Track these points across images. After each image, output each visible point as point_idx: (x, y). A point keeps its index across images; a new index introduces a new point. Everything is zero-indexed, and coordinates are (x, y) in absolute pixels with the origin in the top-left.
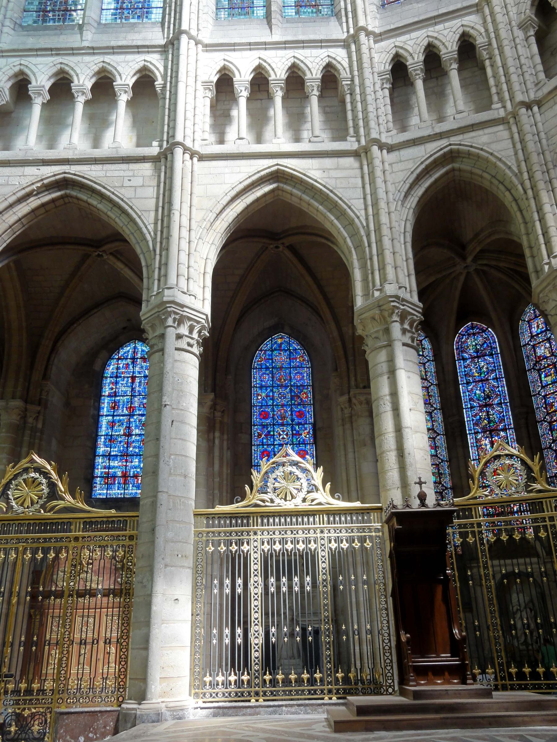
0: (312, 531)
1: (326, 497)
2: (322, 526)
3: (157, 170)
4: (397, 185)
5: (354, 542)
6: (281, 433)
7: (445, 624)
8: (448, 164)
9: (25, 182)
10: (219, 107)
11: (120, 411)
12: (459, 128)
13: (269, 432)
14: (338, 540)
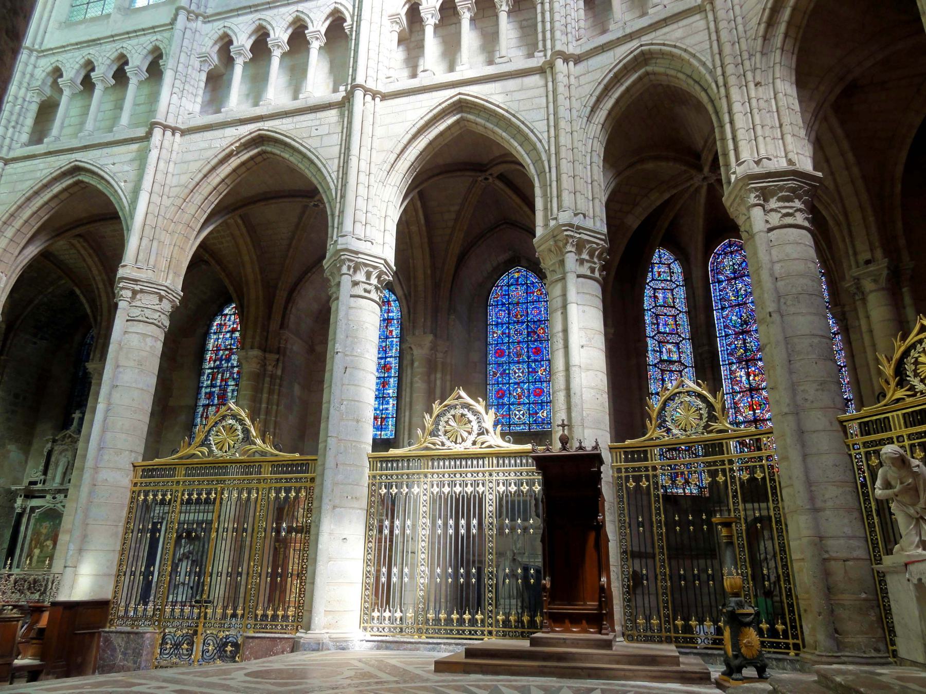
0: (481, 475)
1: (496, 439)
2: (491, 468)
3: (342, 115)
4: (583, 99)
5: (534, 485)
6: (517, 371)
7: (595, 571)
8: (640, 69)
9: (225, 143)
10: (413, 39)
12: (650, 26)
13: (505, 370)
14: (507, 483)
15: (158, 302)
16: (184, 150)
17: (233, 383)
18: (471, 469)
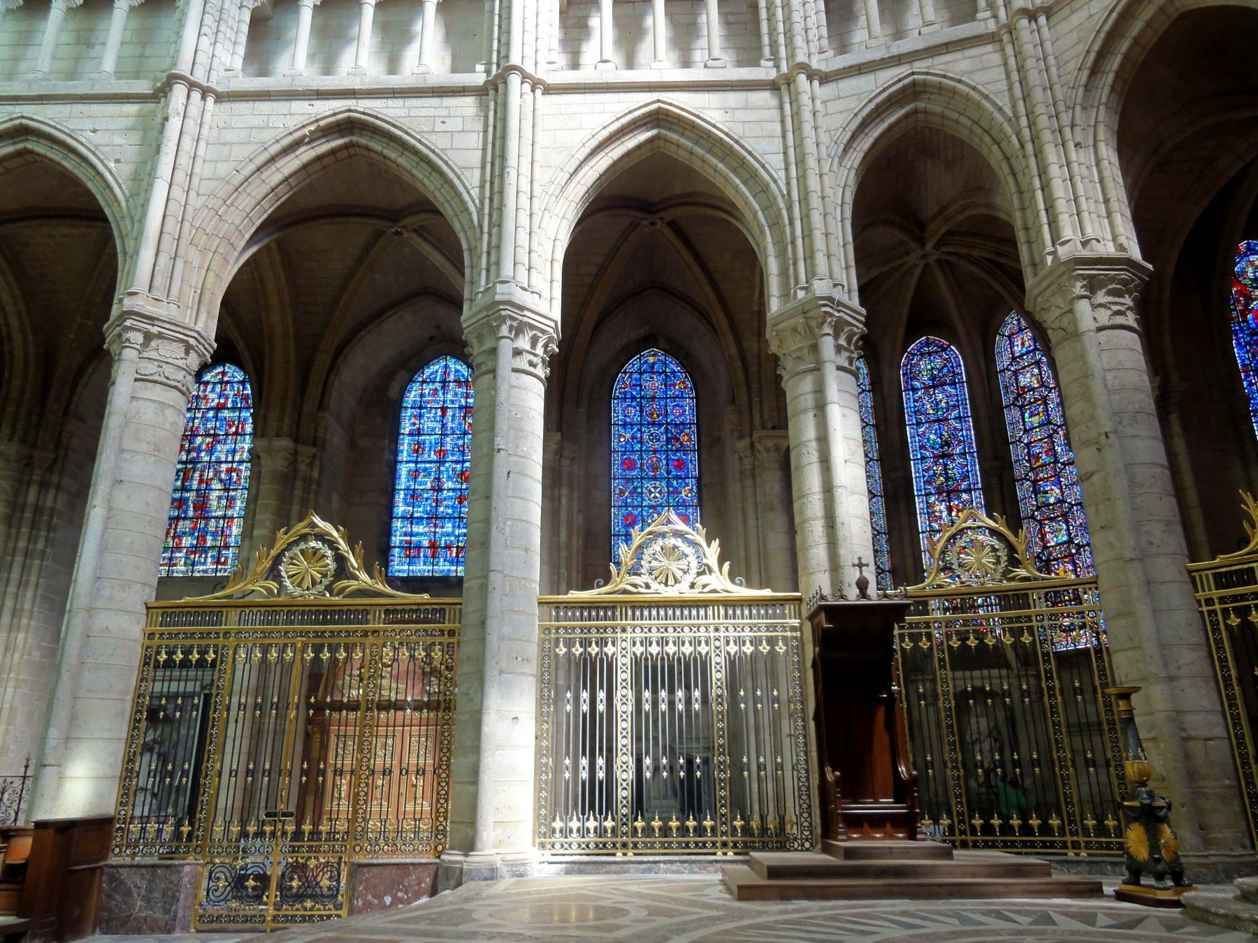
0: (702, 629)
1: (723, 581)
2: (716, 621)
3: (483, 107)
4: (833, 133)
5: (761, 644)
6: (653, 490)
7: (887, 758)
8: (909, 103)
9: (292, 123)
10: (571, 14)
11: (426, 456)
12: (927, 49)
13: (635, 488)
14: (740, 642)
15: (183, 356)
16: (222, 125)
17: (219, 486)
18: (749, 621)
